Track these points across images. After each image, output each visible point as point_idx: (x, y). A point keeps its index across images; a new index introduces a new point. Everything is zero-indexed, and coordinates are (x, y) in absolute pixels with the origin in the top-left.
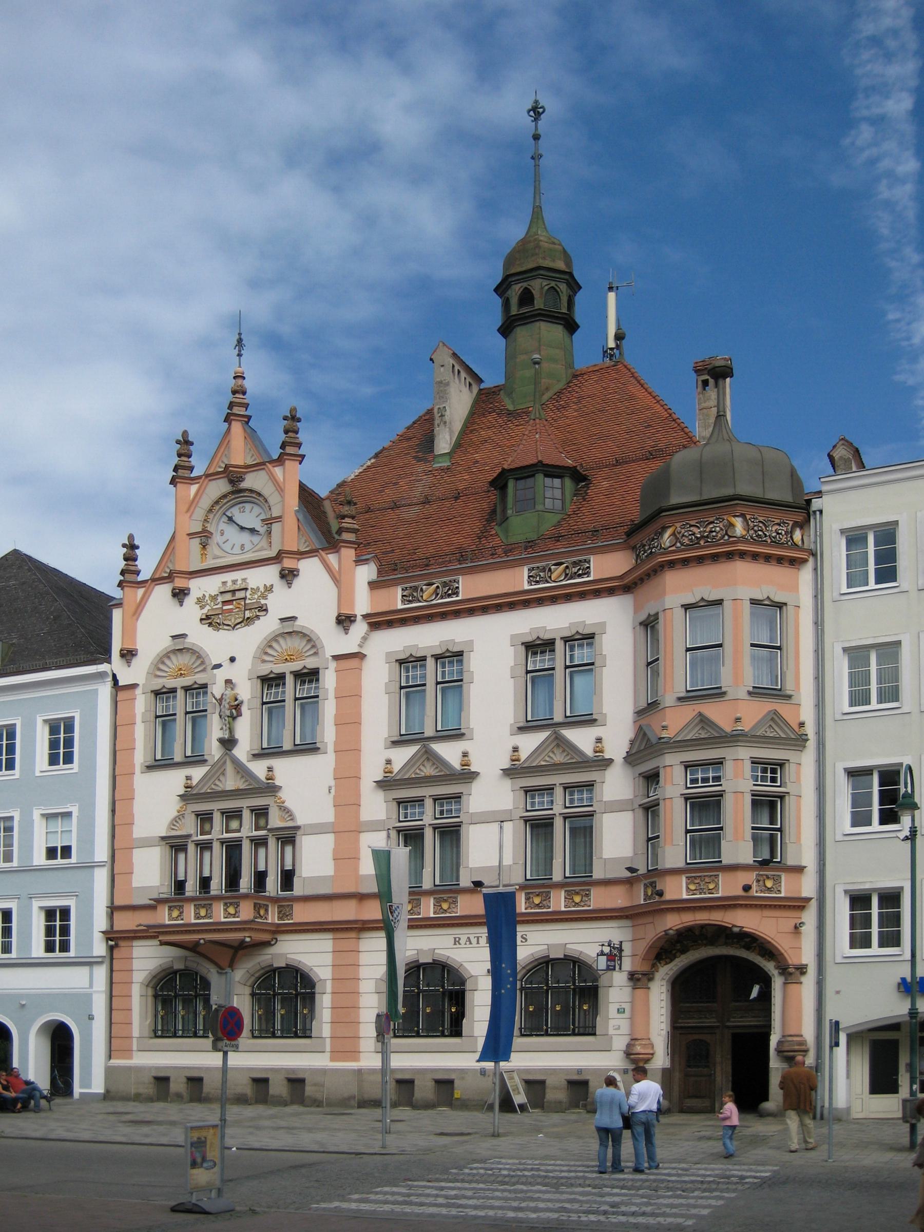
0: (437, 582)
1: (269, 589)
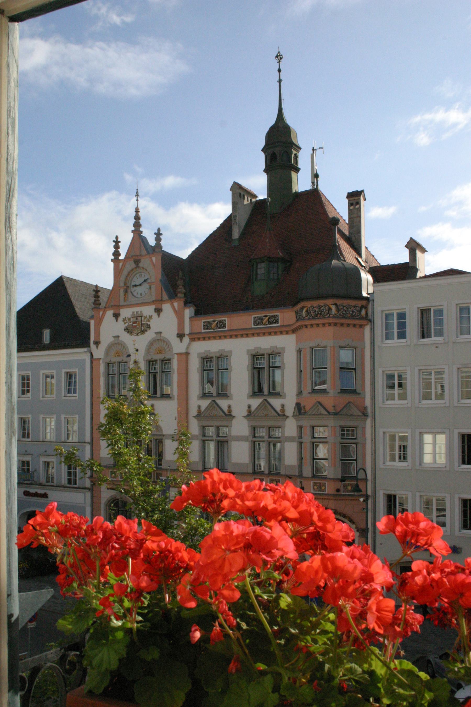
1: (151, 317)
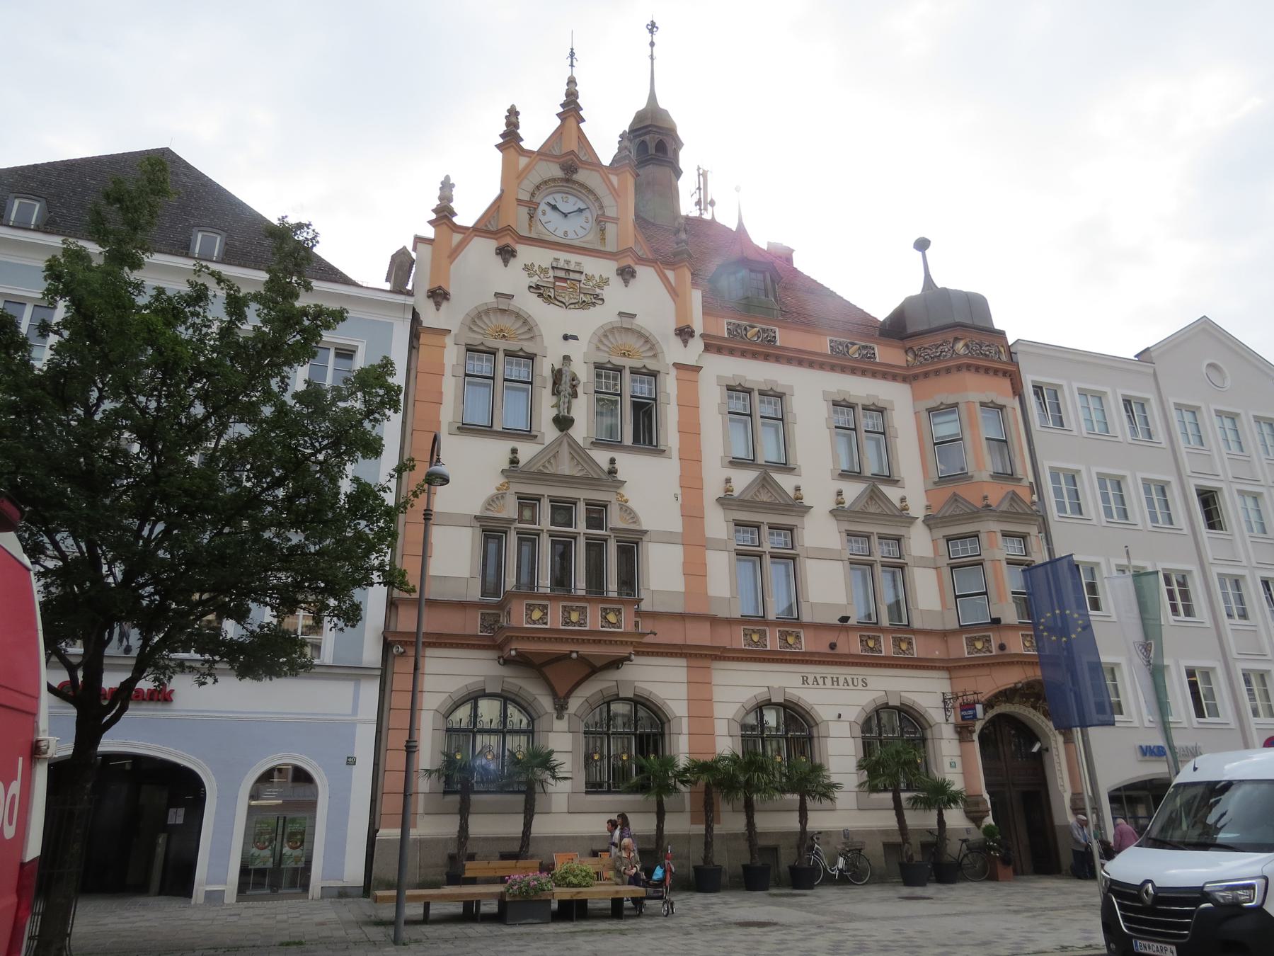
1: (605, 282)
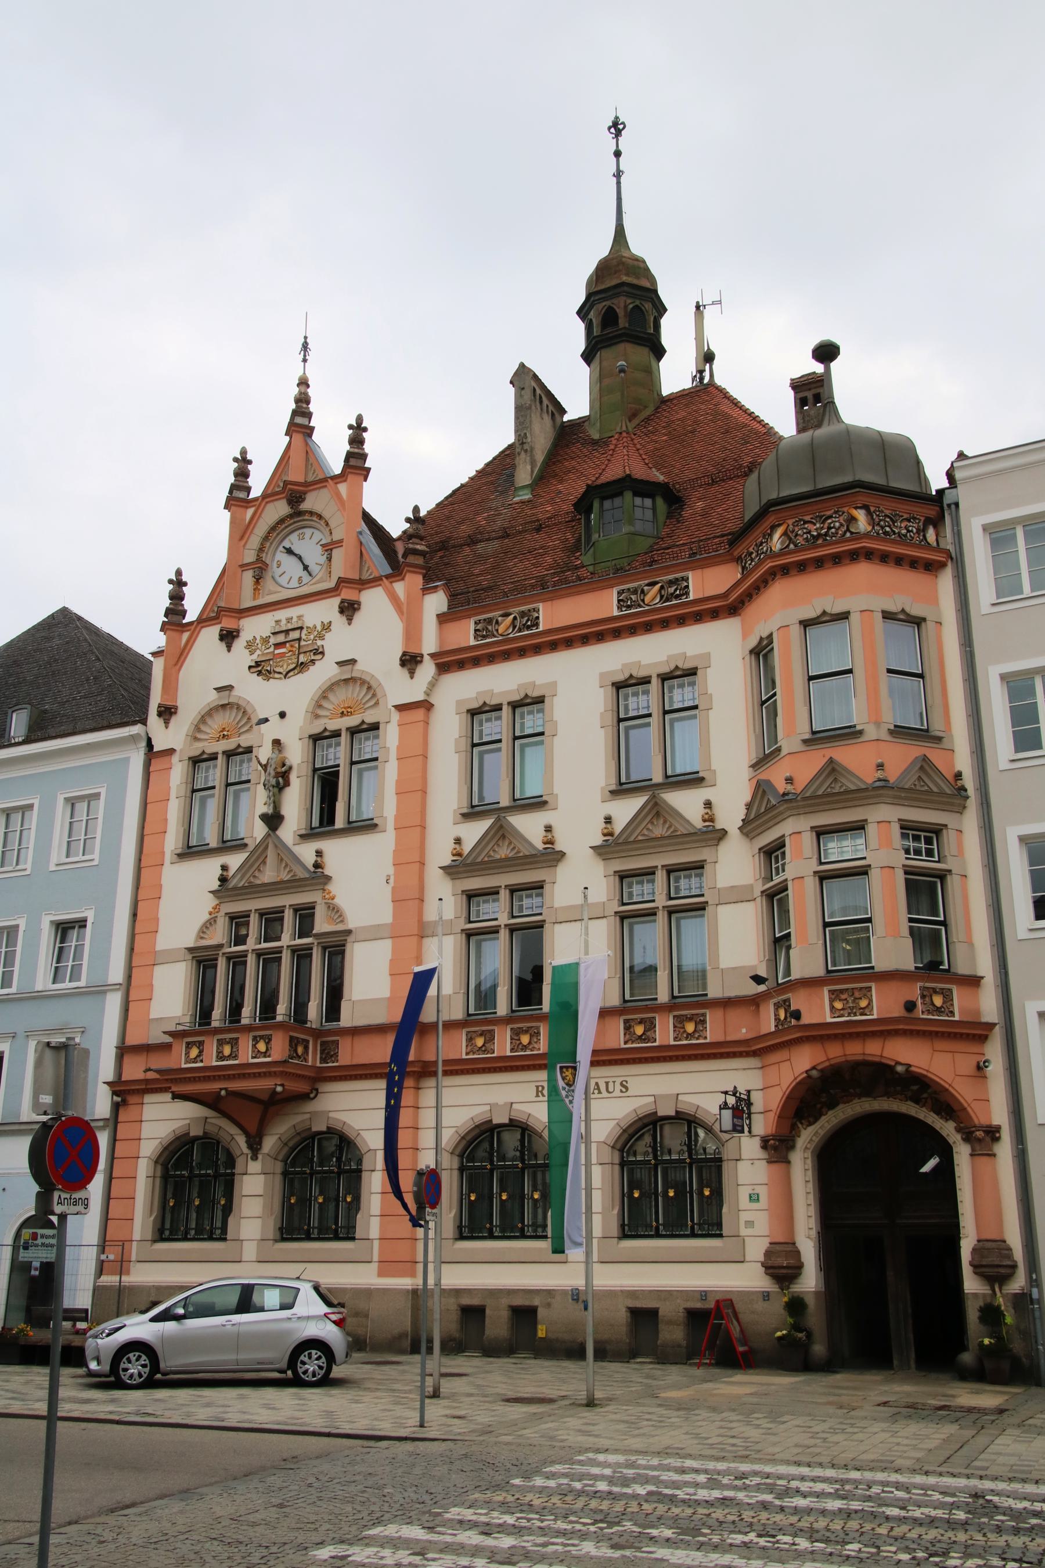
0: (515, 610)
1: (327, 627)
